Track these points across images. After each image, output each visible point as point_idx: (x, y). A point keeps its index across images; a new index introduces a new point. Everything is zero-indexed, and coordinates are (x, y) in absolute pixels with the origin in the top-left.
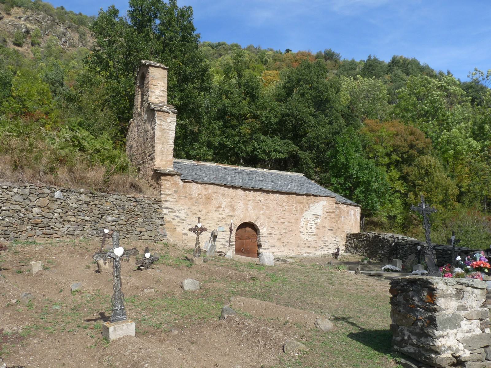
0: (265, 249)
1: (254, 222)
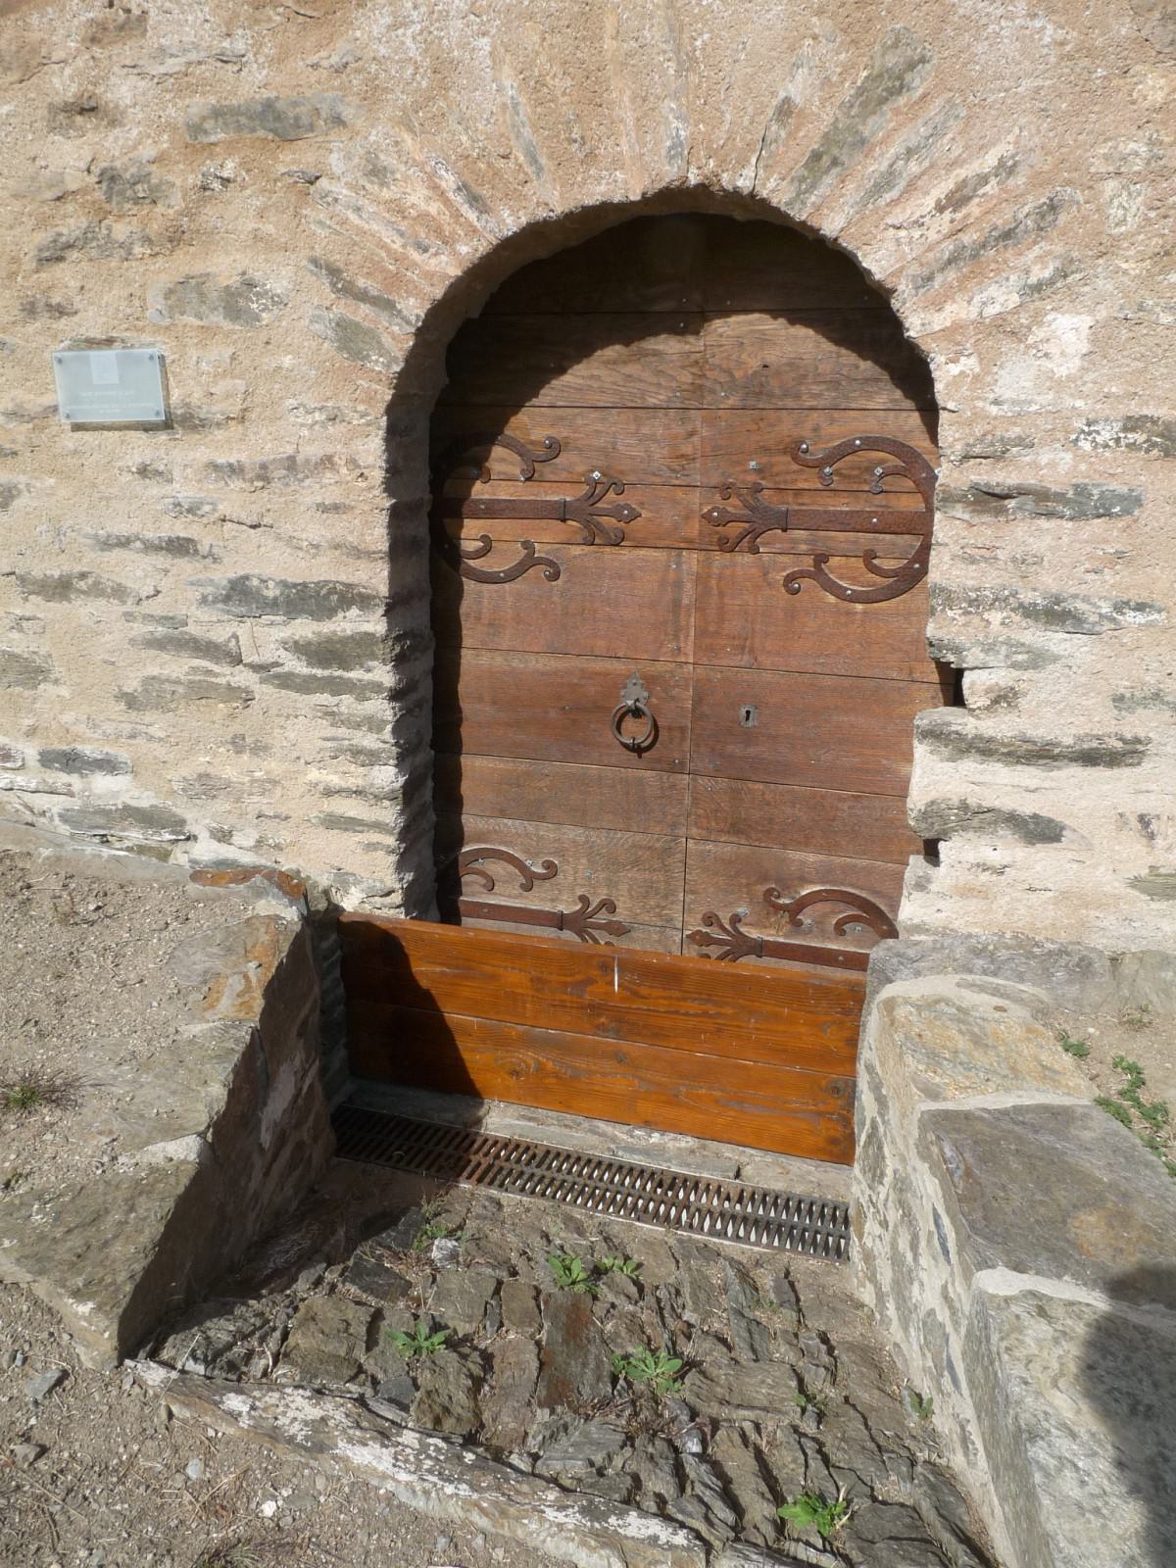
0: (1041, 754)
1: (777, 191)
